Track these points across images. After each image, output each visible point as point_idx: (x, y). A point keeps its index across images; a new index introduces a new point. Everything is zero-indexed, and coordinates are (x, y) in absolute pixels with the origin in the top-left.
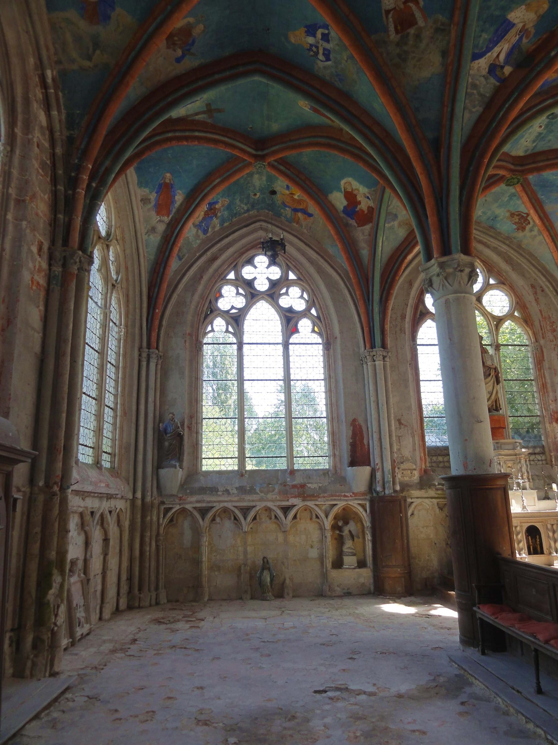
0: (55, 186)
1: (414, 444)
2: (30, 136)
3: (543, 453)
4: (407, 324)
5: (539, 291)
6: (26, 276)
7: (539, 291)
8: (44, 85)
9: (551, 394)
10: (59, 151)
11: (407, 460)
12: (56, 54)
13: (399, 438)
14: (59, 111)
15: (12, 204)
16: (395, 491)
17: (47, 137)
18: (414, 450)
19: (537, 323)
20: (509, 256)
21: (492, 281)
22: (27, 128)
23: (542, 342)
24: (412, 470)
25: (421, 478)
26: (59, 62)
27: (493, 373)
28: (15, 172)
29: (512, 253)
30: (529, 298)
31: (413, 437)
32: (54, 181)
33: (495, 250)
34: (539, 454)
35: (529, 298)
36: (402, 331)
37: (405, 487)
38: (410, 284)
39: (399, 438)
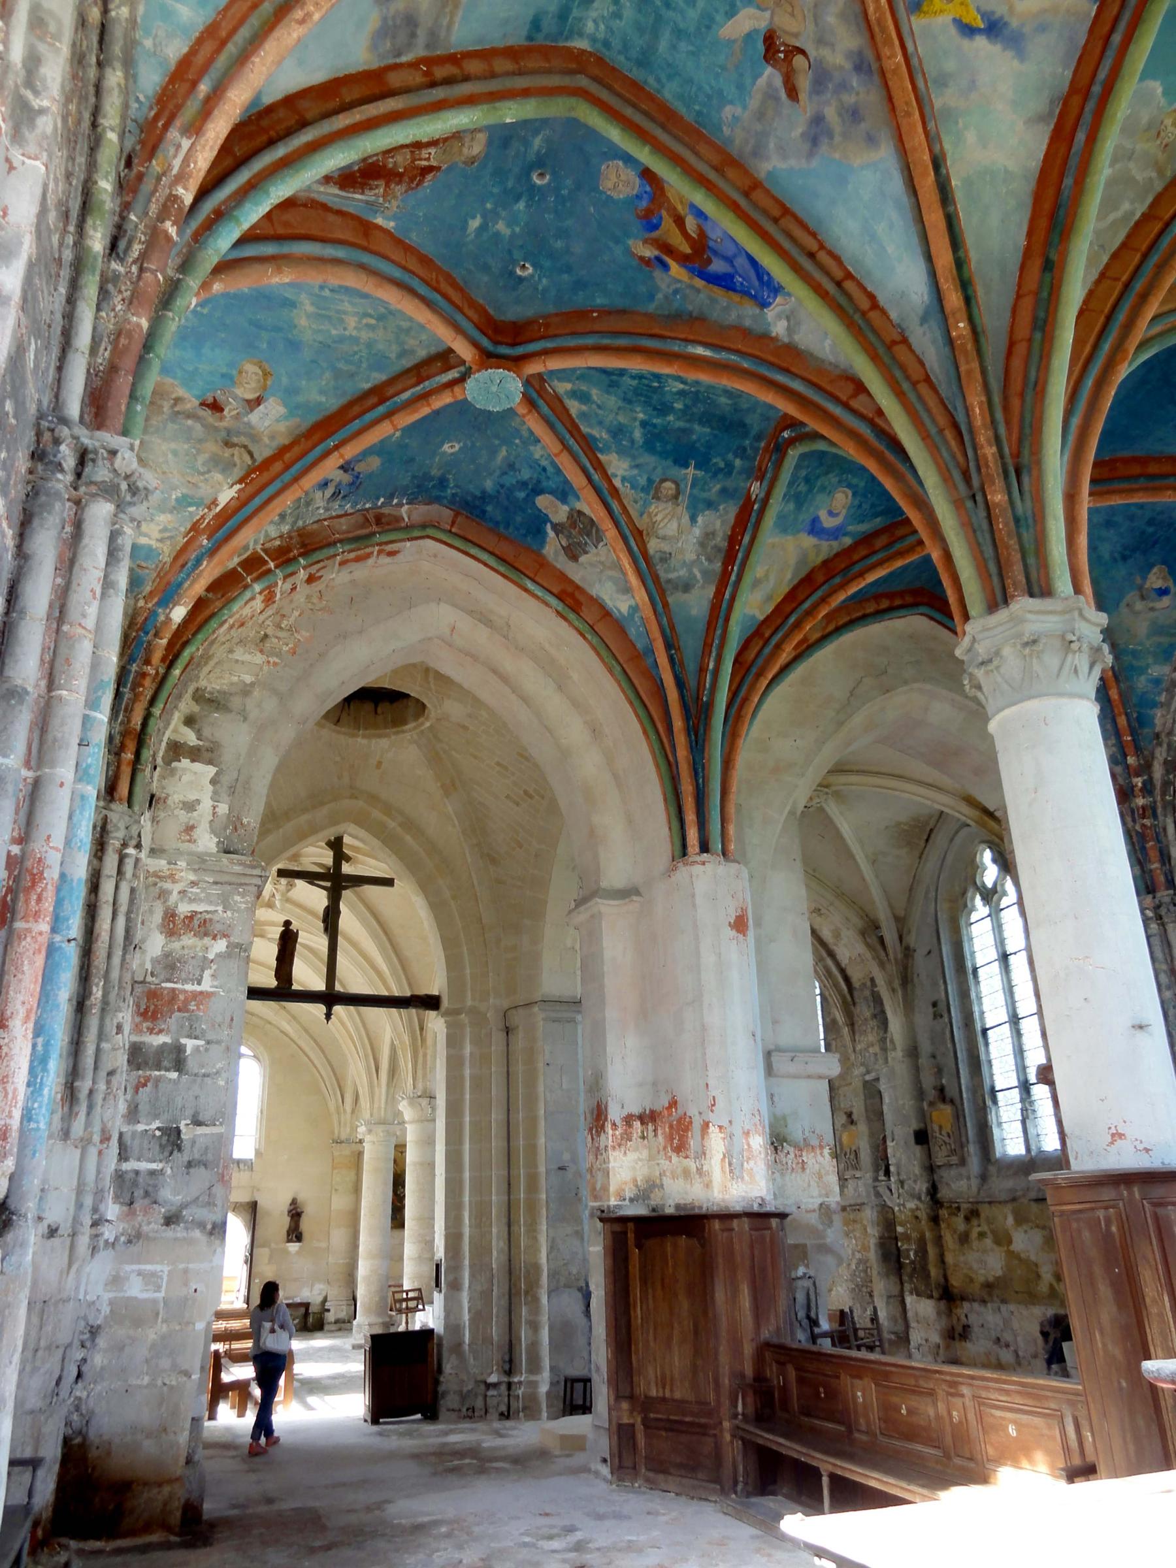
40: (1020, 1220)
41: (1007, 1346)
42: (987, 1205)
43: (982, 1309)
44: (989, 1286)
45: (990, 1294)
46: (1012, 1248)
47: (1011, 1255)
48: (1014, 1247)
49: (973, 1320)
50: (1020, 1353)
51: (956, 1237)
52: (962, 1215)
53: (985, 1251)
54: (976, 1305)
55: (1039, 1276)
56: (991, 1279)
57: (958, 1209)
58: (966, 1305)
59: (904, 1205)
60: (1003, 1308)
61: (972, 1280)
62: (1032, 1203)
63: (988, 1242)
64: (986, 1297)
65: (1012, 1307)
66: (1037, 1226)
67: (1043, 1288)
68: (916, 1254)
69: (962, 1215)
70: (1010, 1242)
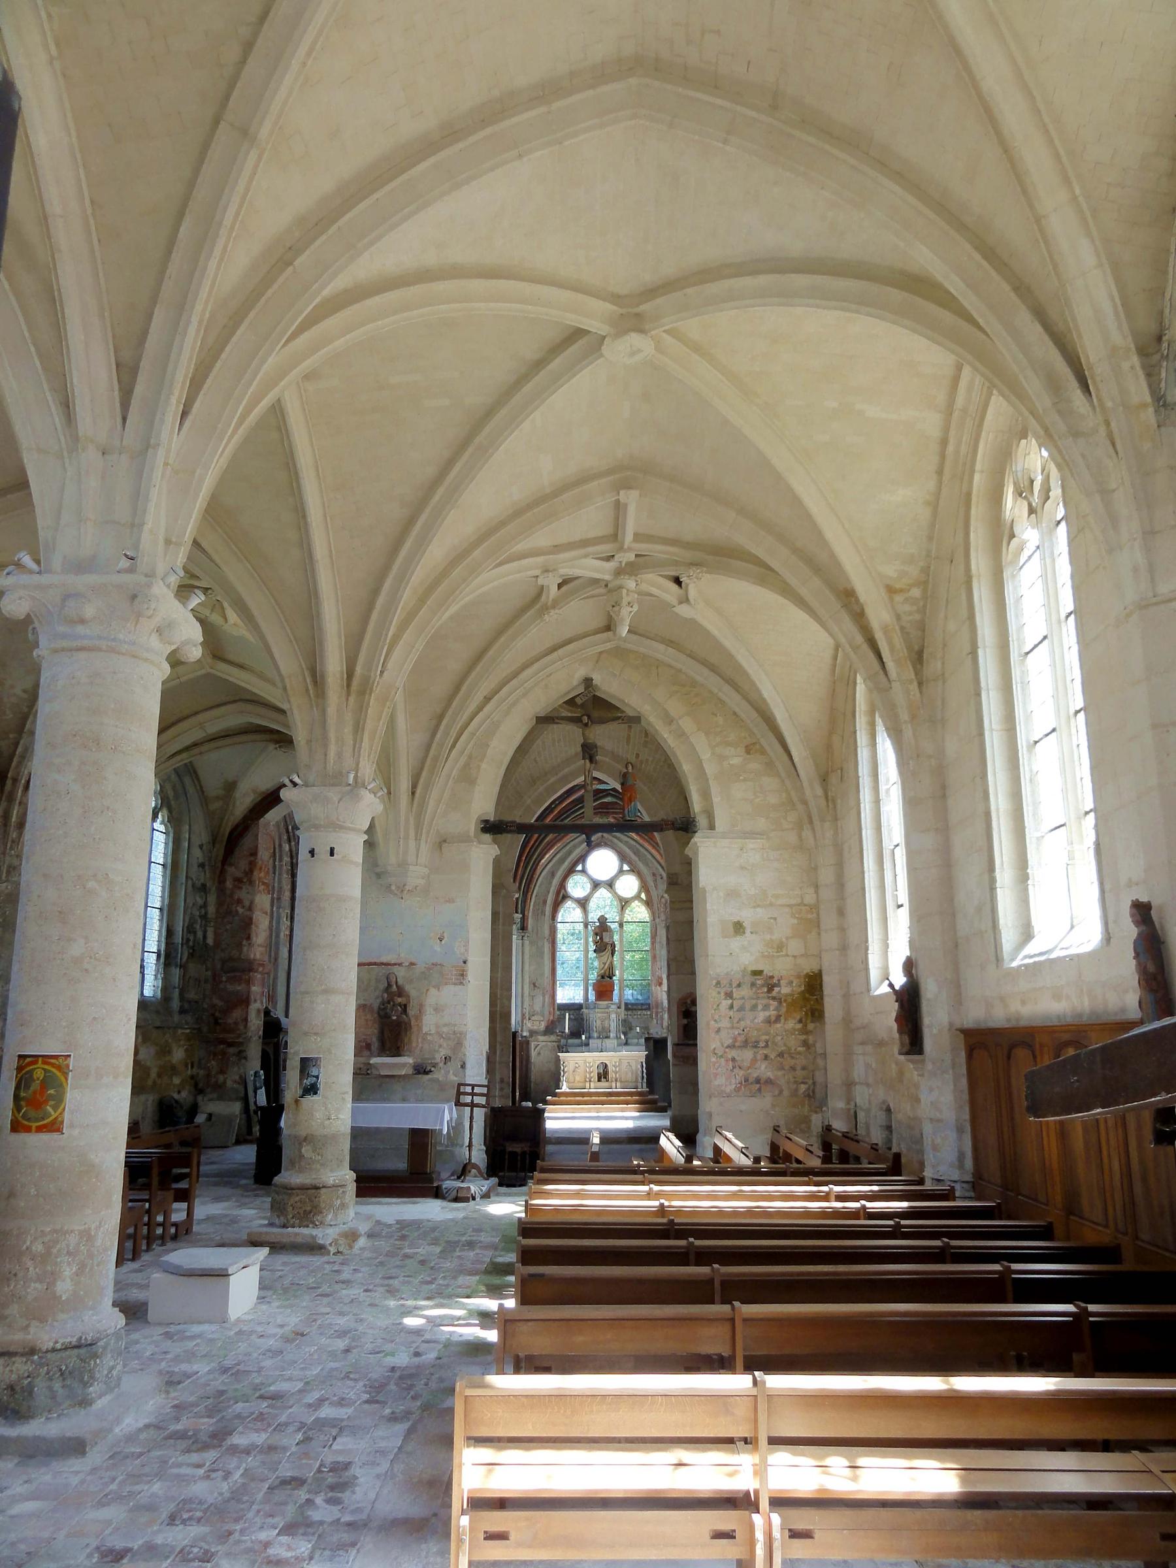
1: (544, 1002)
3: (649, 1009)
4: (548, 909)
5: (658, 878)
7: (658, 878)
8: (288, 832)
9: (658, 963)
11: (537, 1014)
13: (532, 997)
16: (522, 1037)
18: (543, 1006)
19: (655, 906)
20: (638, 849)
21: (626, 867)
23: (657, 920)
24: (540, 1021)
25: (547, 1028)
27: (609, 947)
29: (638, 846)
30: (651, 884)
31: (544, 996)
33: (626, 843)
34: (645, 1010)
35: (651, 884)
36: (543, 913)
37: (533, 1033)
38: (553, 874)
39: (532, 997)
55: (149, 1075)
67: (150, 1082)
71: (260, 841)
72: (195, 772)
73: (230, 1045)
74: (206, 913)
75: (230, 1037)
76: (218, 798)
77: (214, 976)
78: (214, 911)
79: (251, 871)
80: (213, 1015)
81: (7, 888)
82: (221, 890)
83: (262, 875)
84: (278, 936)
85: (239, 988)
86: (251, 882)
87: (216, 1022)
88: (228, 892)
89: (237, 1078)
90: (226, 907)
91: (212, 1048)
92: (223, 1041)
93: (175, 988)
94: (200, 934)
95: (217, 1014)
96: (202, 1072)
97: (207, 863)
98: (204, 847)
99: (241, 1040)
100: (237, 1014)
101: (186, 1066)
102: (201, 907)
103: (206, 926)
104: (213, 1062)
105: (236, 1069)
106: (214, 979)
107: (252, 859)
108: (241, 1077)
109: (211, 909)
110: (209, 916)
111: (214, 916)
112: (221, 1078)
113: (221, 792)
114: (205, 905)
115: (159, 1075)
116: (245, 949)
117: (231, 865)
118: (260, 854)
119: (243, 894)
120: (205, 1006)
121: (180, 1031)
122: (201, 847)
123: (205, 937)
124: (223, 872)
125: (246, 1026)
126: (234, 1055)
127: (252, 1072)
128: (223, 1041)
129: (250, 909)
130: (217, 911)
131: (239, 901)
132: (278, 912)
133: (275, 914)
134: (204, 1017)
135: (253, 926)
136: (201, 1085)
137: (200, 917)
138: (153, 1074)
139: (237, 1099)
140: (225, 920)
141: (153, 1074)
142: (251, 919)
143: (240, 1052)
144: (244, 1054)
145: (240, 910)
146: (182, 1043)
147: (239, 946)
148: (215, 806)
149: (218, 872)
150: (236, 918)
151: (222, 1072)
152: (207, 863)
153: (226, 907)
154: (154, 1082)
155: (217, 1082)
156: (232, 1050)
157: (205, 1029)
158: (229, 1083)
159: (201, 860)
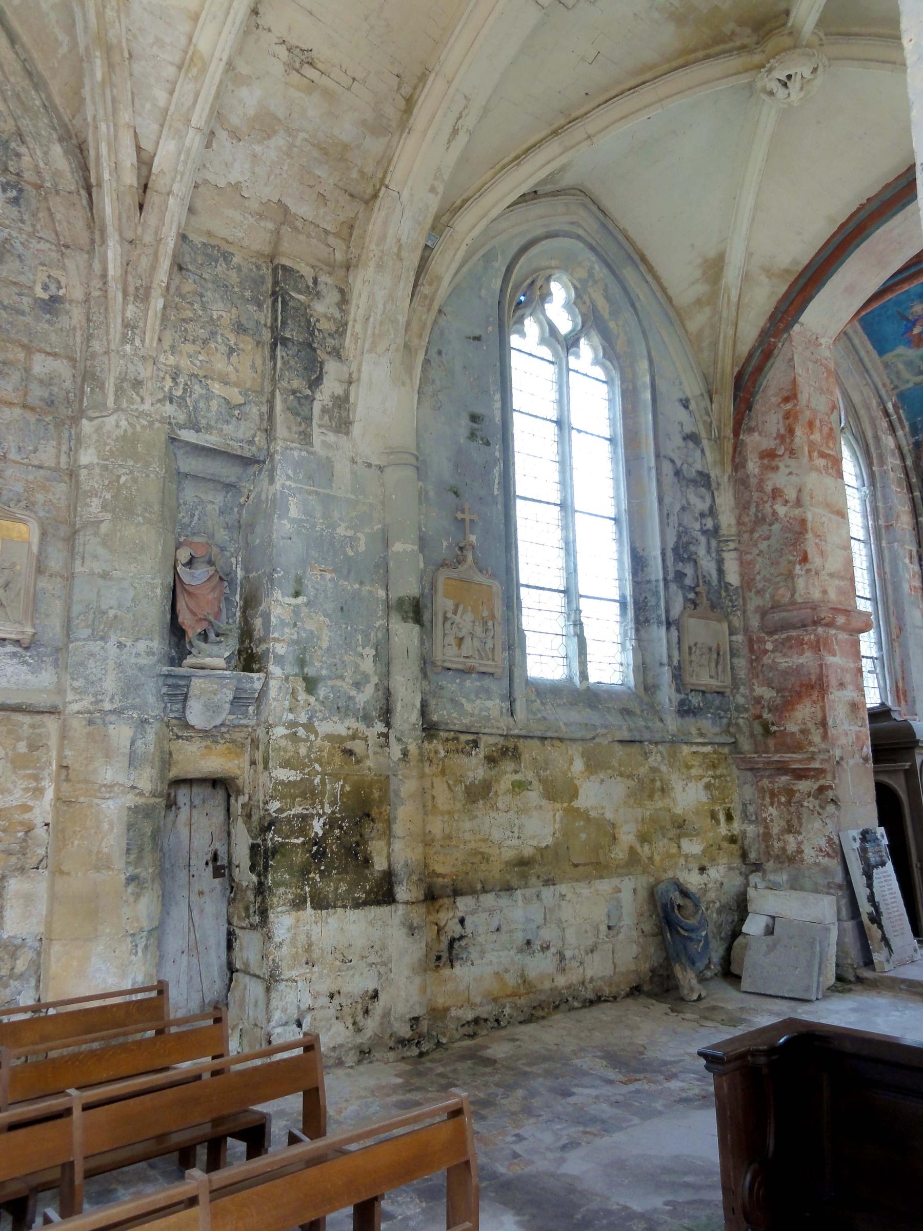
0: (912, 493)
2: (885, 467)
6: (906, 587)
8: (887, 414)
10: (909, 462)
12: (892, 382)
14: (903, 428)
15: (883, 531)
17: (897, 455)
22: (882, 463)
26: (896, 387)
28: (880, 504)
32: (910, 489)
40: (594, 764)
41: (545, 948)
42: (537, 742)
43: (504, 901)
44: (523, 863)
45: (524, 877)
46: (575, 804)
47: (573, 813)
48: (582, 802)
49: (478, 923)
50: (568, 954)
51: (460, 789)
52: (482, 752)
53: (523, 811)
54: (488, 900)
56: (528, 852)
57: (475, 744)
58: (464, 904)
59: (309, 727)
60: (547, 893)
61: (486, 858)
62: (617, 747)
63: (534, 796)
64: (514, 882)
65: (563, 888)
66: (621, 775)
67: (619, 853)
68: (332, 823)
69: (482, 752)
70: (575, 795)
71: (799, 370)
72: (643, 259)
73: (800, 775)
74: (717, 529)
75: (795, 760)
76: (699, 302)
77: (751, 642)
78: (733, 521)
79: (791, 431)
80: (759, 717)
81: (117, 426)
82: (741, 482)
83: (816, 437)
84: (897, 588)
85: (801, 661)
86: (792, 453)
87: (767, 732)
88: (753, 481)
89: (823, 843)
90: (753, 510)
91: (765, 782)
92: (782, 769)
93: (661, 664)
94: (708, 565)
95: (766, 715)
96: (751, 830)
97: (703, 435)
98: (693, 406)
99: (816, 765)
100: (804, 712)
101: (714, 816)
102: (702, 515)
103: (719, 551)
104: (771, 810)
105: (817, 824)
106: (751, 650)
107: (788, 406)
108: (830, 840)
109: (727, 520)
110: (724, 531)
111: (734, 530)
112: (791, 842)
113: (701, 289)
114: (712, 512)
115: (644, 838)
116: (801, 583)
117: (751, 430)
118: (803, 398)
119: (778, 479)
120: (741, 700)
121: (686, 750)
122: (685, 404)
123: (721, 572)
124: (738, 447)
125: (825, 736)
126: (809, 795)
127: (856, 833)
128: (782, 769)
129: (799, 503)
130: (740, 523)
131: (776, 493)
132: (891, 549)
133: (886, 553)
134: (741, 721)
135: (810, 536)
136: (753, 856)
137: (704, 532)
138: (627, 836)
139: (829, 888)
140: (756, 535)
141: (627, 836)
142: (803, 522)
143: (822, 789)
144: (830, 794)
145: (781, 510)
146: (694, 772)
147: (790, 576)
148: (697, 322)
149: (728, 447)
150: (776, 527)
151: (790, 829)
152: (703, 435)
153: (753, 510)
154: (632, 850)
155: (784, 849)
156: (804, 786)
157: (746, 745)
158: (809, 854)
159: (688, 429)
